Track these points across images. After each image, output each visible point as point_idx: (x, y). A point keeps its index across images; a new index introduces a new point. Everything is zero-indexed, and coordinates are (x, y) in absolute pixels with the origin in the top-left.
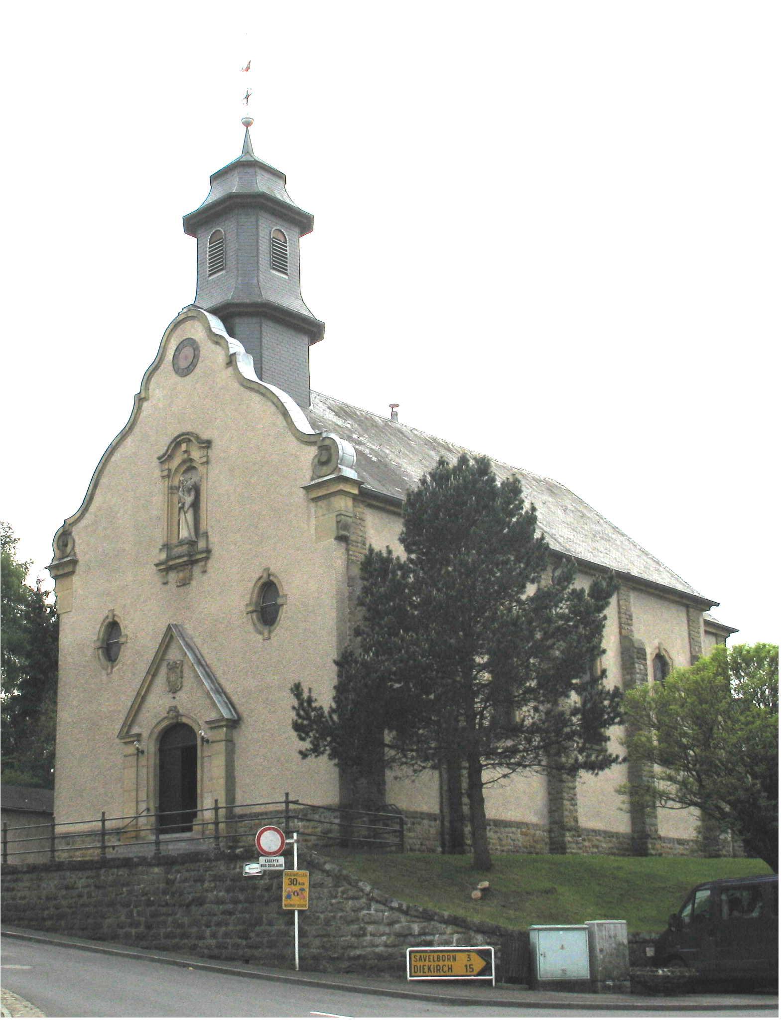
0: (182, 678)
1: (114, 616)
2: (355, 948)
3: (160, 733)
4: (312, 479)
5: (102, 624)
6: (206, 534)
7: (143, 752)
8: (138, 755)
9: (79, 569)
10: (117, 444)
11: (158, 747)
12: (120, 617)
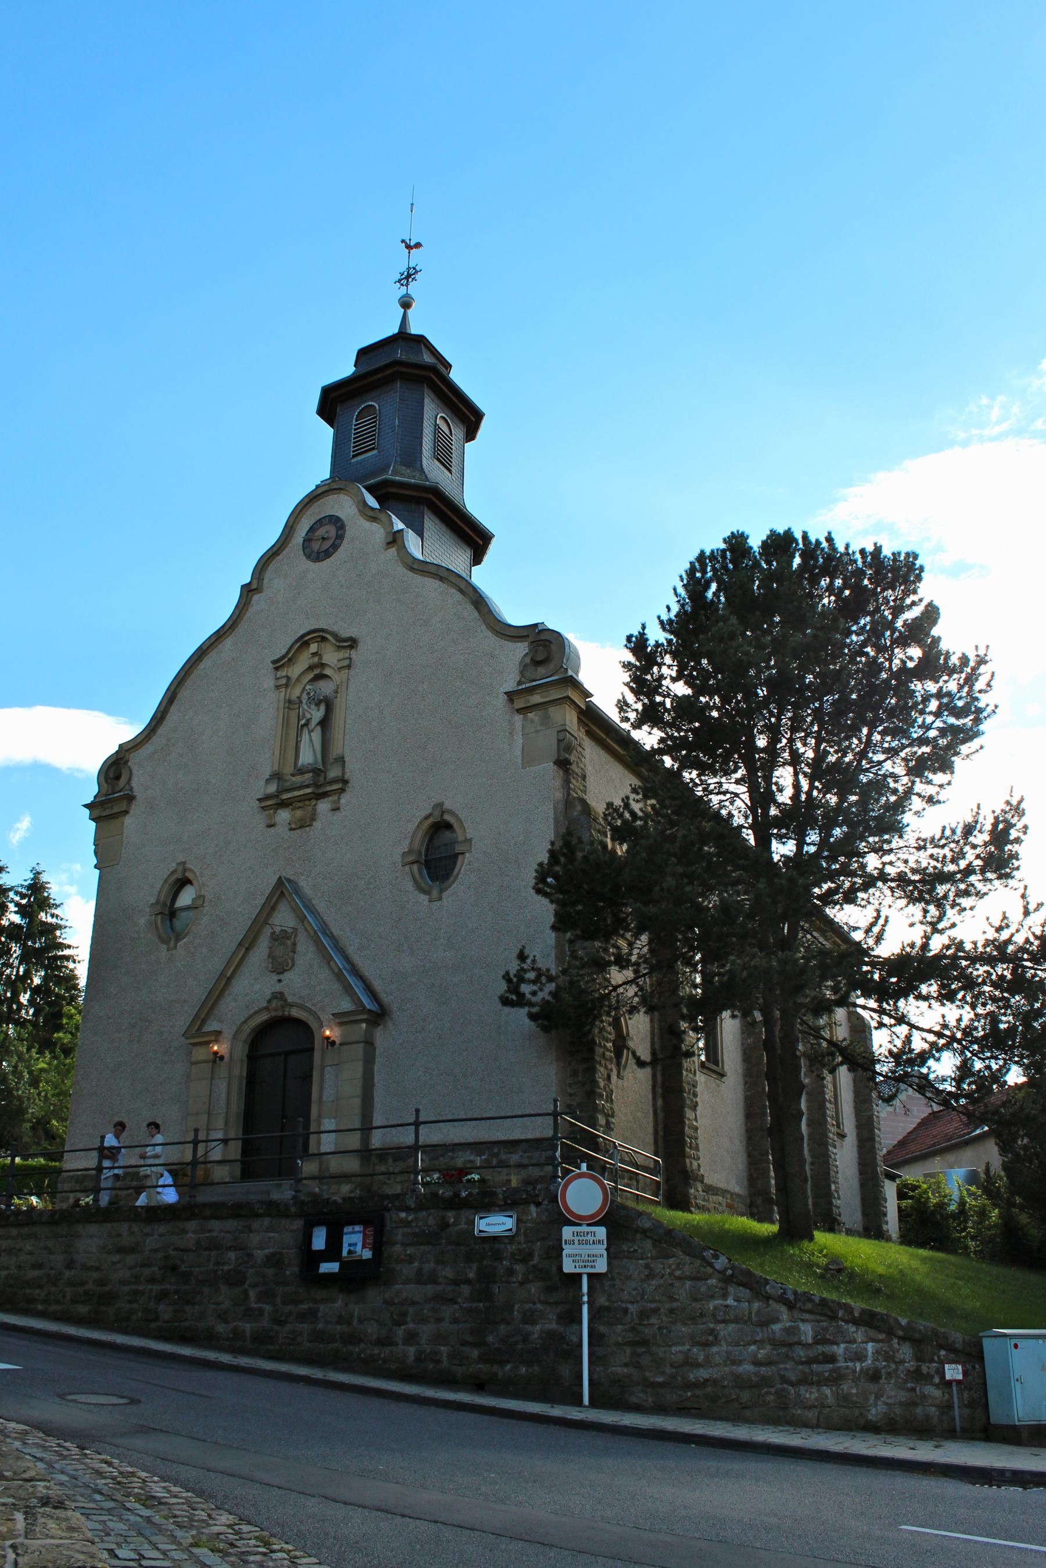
0: (294, 952)
1: (185, 870)
2: (698, 1366)
3: (253, 1030)
4: (519, 683)
5: (166, 881)
6: (341, 760)
7: (222, 1058)
8: (214, 1062)
9: (136, 809)
10: (208, 648)
11: (247, 1051)
12: (195, 873)
